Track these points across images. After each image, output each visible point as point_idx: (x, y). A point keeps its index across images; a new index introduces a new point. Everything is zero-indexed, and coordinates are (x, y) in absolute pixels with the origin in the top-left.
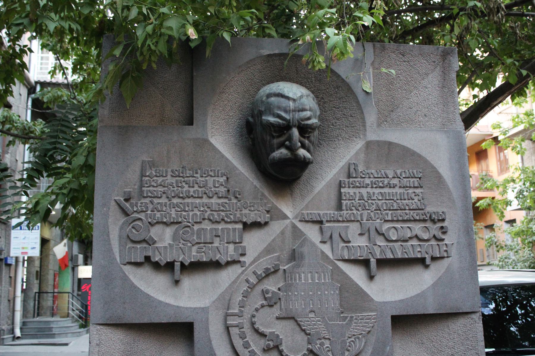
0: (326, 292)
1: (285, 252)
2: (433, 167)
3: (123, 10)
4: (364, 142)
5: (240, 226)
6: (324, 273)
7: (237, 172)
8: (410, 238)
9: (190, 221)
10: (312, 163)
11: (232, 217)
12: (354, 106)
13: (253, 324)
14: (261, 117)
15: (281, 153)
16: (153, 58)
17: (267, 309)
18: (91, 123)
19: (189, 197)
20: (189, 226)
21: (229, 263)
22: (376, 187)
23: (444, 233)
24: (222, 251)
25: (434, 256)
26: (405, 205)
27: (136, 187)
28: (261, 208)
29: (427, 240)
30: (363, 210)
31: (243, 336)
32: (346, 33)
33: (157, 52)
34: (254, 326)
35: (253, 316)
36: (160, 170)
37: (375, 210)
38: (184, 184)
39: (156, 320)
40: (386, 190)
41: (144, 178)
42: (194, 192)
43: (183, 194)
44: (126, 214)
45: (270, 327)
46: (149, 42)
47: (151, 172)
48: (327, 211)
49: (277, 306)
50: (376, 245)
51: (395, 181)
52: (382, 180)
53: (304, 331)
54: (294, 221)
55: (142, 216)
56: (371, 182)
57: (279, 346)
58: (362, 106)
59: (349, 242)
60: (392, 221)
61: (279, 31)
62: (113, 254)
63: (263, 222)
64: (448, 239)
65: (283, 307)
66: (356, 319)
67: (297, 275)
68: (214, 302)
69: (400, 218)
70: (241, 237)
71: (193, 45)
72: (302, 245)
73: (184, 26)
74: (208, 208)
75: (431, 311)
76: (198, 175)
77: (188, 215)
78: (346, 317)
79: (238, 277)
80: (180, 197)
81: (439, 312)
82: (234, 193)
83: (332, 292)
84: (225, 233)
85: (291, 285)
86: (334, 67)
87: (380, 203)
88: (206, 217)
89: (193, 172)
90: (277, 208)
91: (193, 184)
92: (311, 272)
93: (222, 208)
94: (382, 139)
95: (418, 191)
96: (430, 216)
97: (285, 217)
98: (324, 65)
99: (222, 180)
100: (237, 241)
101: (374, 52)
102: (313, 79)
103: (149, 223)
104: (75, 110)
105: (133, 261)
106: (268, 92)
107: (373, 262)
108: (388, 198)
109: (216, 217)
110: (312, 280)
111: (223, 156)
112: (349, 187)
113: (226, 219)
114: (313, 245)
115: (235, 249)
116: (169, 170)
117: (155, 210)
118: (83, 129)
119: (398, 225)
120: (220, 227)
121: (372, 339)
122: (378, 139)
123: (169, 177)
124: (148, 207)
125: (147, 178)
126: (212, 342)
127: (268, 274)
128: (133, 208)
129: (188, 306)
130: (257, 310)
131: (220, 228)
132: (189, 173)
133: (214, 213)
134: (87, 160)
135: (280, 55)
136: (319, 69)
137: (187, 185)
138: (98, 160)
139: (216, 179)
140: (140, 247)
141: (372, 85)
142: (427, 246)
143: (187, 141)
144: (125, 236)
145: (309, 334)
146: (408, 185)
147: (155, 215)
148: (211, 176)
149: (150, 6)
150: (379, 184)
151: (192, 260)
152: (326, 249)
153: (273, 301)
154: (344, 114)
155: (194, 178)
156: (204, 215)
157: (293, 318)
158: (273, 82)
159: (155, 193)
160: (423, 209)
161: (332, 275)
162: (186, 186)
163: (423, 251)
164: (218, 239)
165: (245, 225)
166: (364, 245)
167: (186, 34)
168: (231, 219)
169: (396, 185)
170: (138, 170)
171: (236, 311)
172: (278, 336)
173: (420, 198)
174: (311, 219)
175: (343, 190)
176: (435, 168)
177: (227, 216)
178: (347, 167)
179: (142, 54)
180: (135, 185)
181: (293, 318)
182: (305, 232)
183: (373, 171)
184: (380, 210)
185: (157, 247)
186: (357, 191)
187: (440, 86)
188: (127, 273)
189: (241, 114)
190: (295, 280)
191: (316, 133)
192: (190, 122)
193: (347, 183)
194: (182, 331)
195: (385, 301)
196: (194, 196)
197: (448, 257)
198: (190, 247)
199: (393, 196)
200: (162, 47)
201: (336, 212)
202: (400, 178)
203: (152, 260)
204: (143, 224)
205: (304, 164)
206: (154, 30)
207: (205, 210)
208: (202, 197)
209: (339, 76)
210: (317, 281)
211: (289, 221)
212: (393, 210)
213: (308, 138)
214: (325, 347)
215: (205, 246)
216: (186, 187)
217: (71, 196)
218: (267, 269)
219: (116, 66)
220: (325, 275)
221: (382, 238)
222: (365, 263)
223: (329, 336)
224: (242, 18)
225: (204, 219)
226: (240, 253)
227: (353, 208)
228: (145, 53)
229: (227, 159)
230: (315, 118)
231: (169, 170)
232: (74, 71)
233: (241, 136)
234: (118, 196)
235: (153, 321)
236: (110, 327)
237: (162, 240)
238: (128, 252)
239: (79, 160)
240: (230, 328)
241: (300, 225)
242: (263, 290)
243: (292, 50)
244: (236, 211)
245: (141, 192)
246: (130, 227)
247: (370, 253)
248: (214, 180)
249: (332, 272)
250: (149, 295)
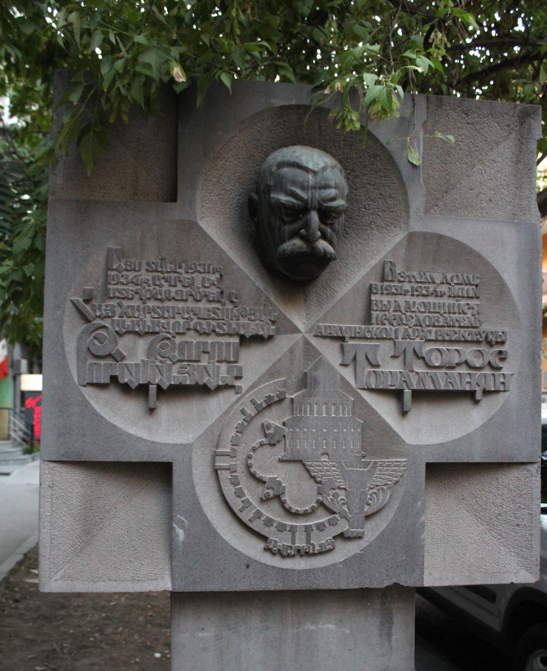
0: (345, 430)
1: (293, 376)
2: (495, 271)
3: (82, 36)
4: (406, 234)
5: (236, 340)
6: (342, 404)
7: (234, 267)
8: (458, 364)
9: (171, 331)
10: (335, 259)
11: (225, 327)
12: (394, 183)
13: (248, 467)
14: (269, 194)
15: (294, 244)
16: (123, 108)
17: (267, 449)
18: (37, 191)
19: (169, 300)
20: (169, 338)
21: (219, 388)
22: (418, 295)
23: (503, 360)
24: (211, 373)
25: (487, 389)
26: (454, 320)
27: (99, 284)
28: (264, 318)
29: (480, 368)
30: (399, 325)
31: (235, 482)
32: (391, 81)
33: (129, 98)
34: (250, 469)
35: (249, 457)
36: (131, 262)
37: (414, 326)
38: (163, 282)
39: (125, 458)
40: (431, 300)
41: (110, 273)
42: (176, 293)
43: (161, 294)
44: (86, 319)
45: (270, 472)
46: (118, 84)
47: (120, 265)
48: (352, 324)
49: (280, 446)
50: (413, 371)
51: (444, 288)
52: (426, 285)
53: (314, 478)
54: (306, 336)
55: (107, 323)
56: (412, 287)
57: (281, 496)
58: (407, 184)
59: (378, 366)
60: (436, 341)
61: (297, 70)
62: (70, 372)
63: (266, 337)
64: (507, 368)
65: (287, 447)
66: (381, 465)
67: (308, 407)
68: (199, 437)
69: (447, 338)
70: (237, 355)
71: (178, 89)
72: (316, 368)
73: (167, 61)
74: (195, 314)
75: (478, 460)
76: (182, 271)
77: (168, 323)
78: (369, 463)
79: (230, 407)
80: (157, 299)
81: (487, 461)
82: (230, 295)
83: (353, 431)
84: (216, 348)
85: (300, 419)
86: (370, 127)
87: (421, 316)
88: (192, 327)
89: (175, 265)
90: (285, 318)
91: (175, 282)
92: (326, 403)
93: (213, 315)
94: (430, 230)
95: (472, 302)
96: (486, 337)
97: (296, 330)
98: (358, 125)
99: (214, 277)
100: (232, 359)
101: (427, 108)
102: (342, 142)
103: (117, 332)
104: (16, 171)
105: (95, 381)
106: (279, 159)
107: (407, 393)
108: (432, 310)
109: (205, 327)
110: (327, 414)
111: (216, 245)
112: (382, 294)
113: (217, 330)
114: (331, 368)
115: (229, 371)
116: (144, 262)
117: (124, 315)
118: (26, 197)
119: (443, 347)
120: (210, 340)
121: (400, 491)
122: (424, 230)
123: (143, 271)
124: (114, 311)
125: (115, 273)
126: (196, 488)
127: (270, 403)
128: (95, 311)
129: (166, 442)
130: (254, 450)
131: (210, 342)
132: (170, 267)
133: (202, 321)
134: (33, 244)
135: (298, 107)
136: (351, 130)
137: (167, 284)
138: (48, 247)
139: (207, 276)
140: (104, 364)
141: (422, 155)
142: (479, 376)
143: (168, 224)
144: (84, 348)
145: (320, 483)
146: (460, 294)
147: (124, 321)
148: (200, 272)
149: (119, 31)
150: (422, 291)
151: (173, 383)
152: (347, 374)
153: (276, 438)
154: (381, 194)
155: (177, 275)
156: (189, 325)
157: (300, 461)
158: (286, 146)
159: (124, 292)
160: (477, 327)
161: (353, 408)
162: (166, 284)
163: (474, 382)
164: (206, 356)
165: (242, 338)
166: (397, 370)
167: (168, 73)
168: (224, 330)
169: (444, 294)
170: (102, 261)
171: (227, 451)
172: (280, 483)
173: (475, 312)
174: (330, 333)
175: (373, 298)
176: (497, 273)
177: (219, 326)
178: (380, 266)
179: (108, 100)
180: (98, 281)
181: (300, 461)
182: (320, 351)
183: (415, 273)
184: (421, 326)
185: (126, 365)
186: (392, 299)
187: (513, 160)
188: (87, 397)
189: (242, 188)
190: (305, 413)
191: (342, 218)
192: (174, 199)
193: (379, 288)
194: (157, 473)
196: (177, 298)
197: (504, 391)
198: (170, 366)
199: (439, 307)
200: (136, 94)
201: (363, 327)
202: (450, 284)
203: (121, 381)
204: (108, 334)
205: (325, 260)
206: (125, 67)
207: (190, 317)
208: (186, 300)
209: (376, 140)
210: (333, 415)
211: (301, 335)
212: (438, 326)
213: (331, 225)
214: (339, 499)
215: (189, 365)
216: (166, 286)
217: (12, 290)
218: (269, 397)
219: (73, 117)
220: (344, 409)
221: (421, 362)
222: (397, 394)
223: (346, 485)
224: (248, 52)
225: (188, 329)
226: (235, 375)
227: (386, 322)
228: (112, 100)
229: (221, 250)
230: (342, 198)
231: (144, 262)
232: (13, 112)
233: (241, 218)
234: (75, 295)
235: (121, 460)
236: (65, 466)
237: (134, 355)
238: (89, 370)
239: (22, 243)
240: (219, 472)
241: (314, 341)
242: (263, 424)
243: (315, 100)
244: (232, 320)
245: (106, 291)
246: (91, 337)
247: (405, 381)
248: (203, 278)
249: (354, 404)
250: (115, 426)
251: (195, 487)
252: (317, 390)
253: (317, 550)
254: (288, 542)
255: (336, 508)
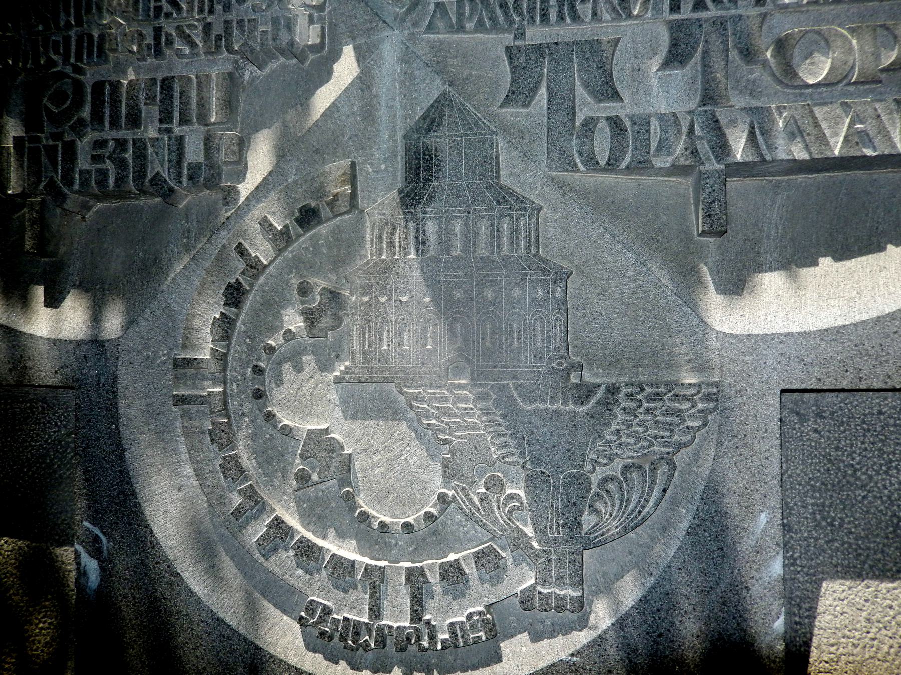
45: (311, 415)
195: (756, 331)
251: (124, 451)
252: (435, 184)
253: (443, 642)
254: (360, 613)
255: (495, 522)
